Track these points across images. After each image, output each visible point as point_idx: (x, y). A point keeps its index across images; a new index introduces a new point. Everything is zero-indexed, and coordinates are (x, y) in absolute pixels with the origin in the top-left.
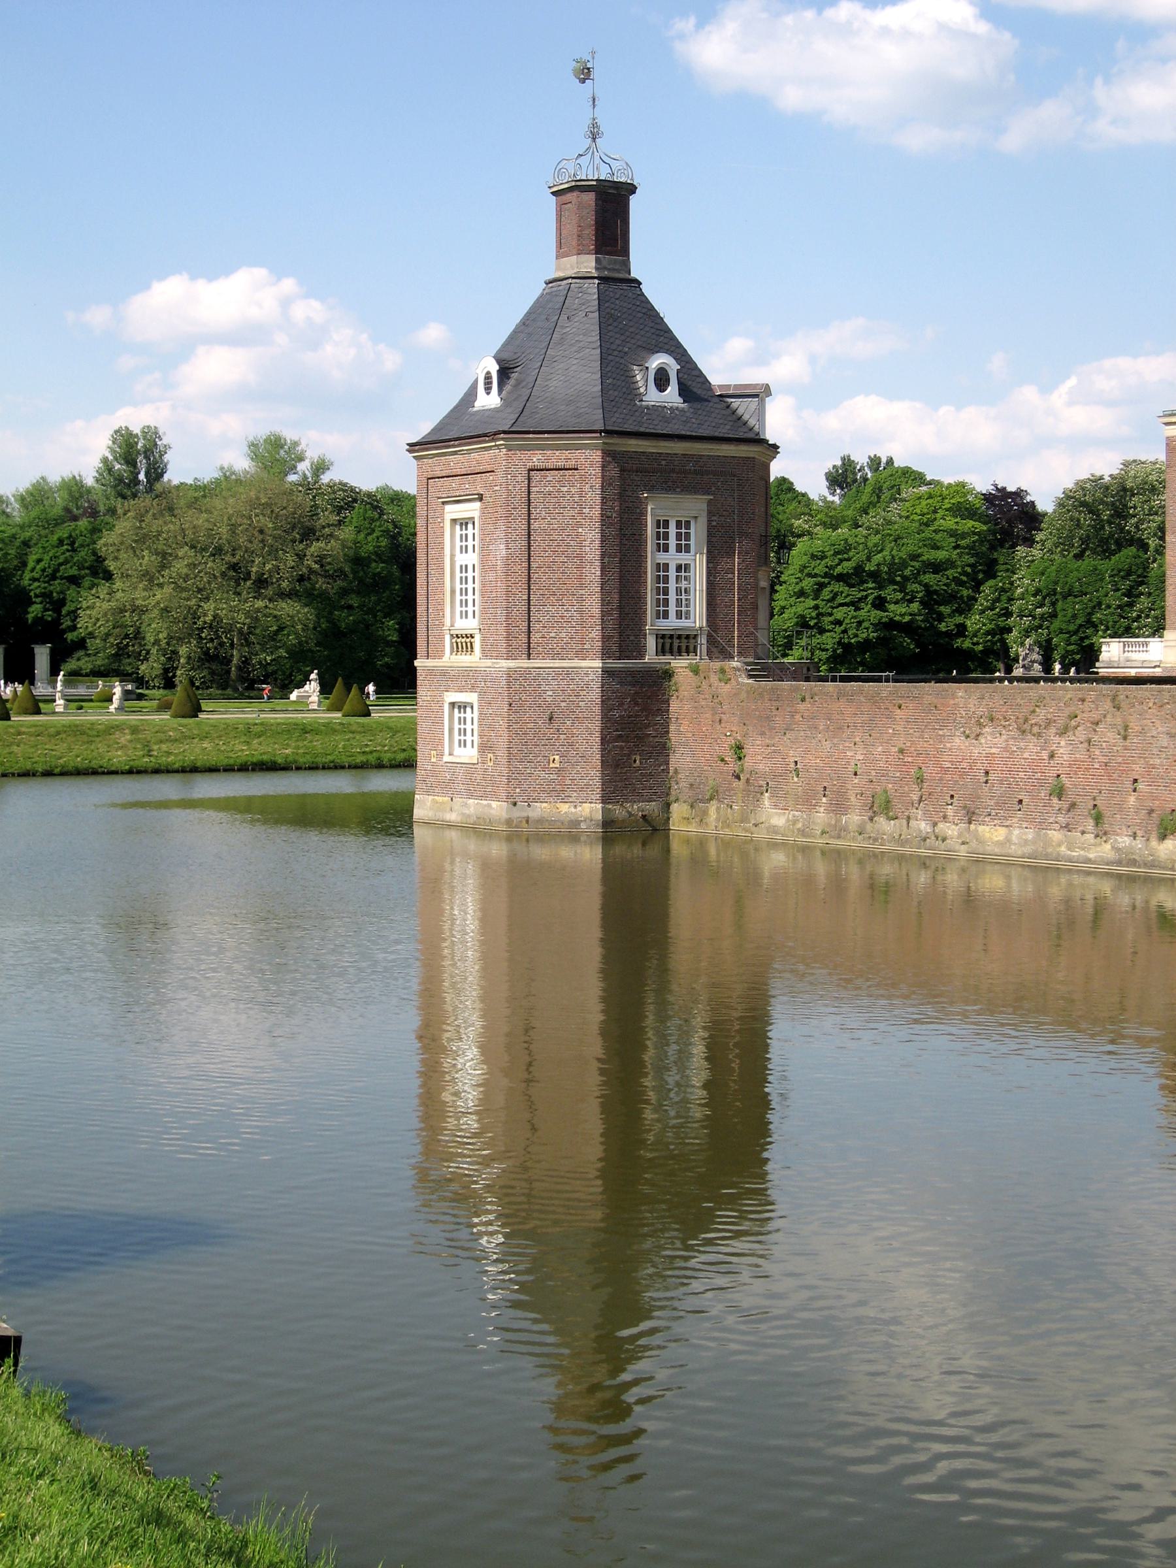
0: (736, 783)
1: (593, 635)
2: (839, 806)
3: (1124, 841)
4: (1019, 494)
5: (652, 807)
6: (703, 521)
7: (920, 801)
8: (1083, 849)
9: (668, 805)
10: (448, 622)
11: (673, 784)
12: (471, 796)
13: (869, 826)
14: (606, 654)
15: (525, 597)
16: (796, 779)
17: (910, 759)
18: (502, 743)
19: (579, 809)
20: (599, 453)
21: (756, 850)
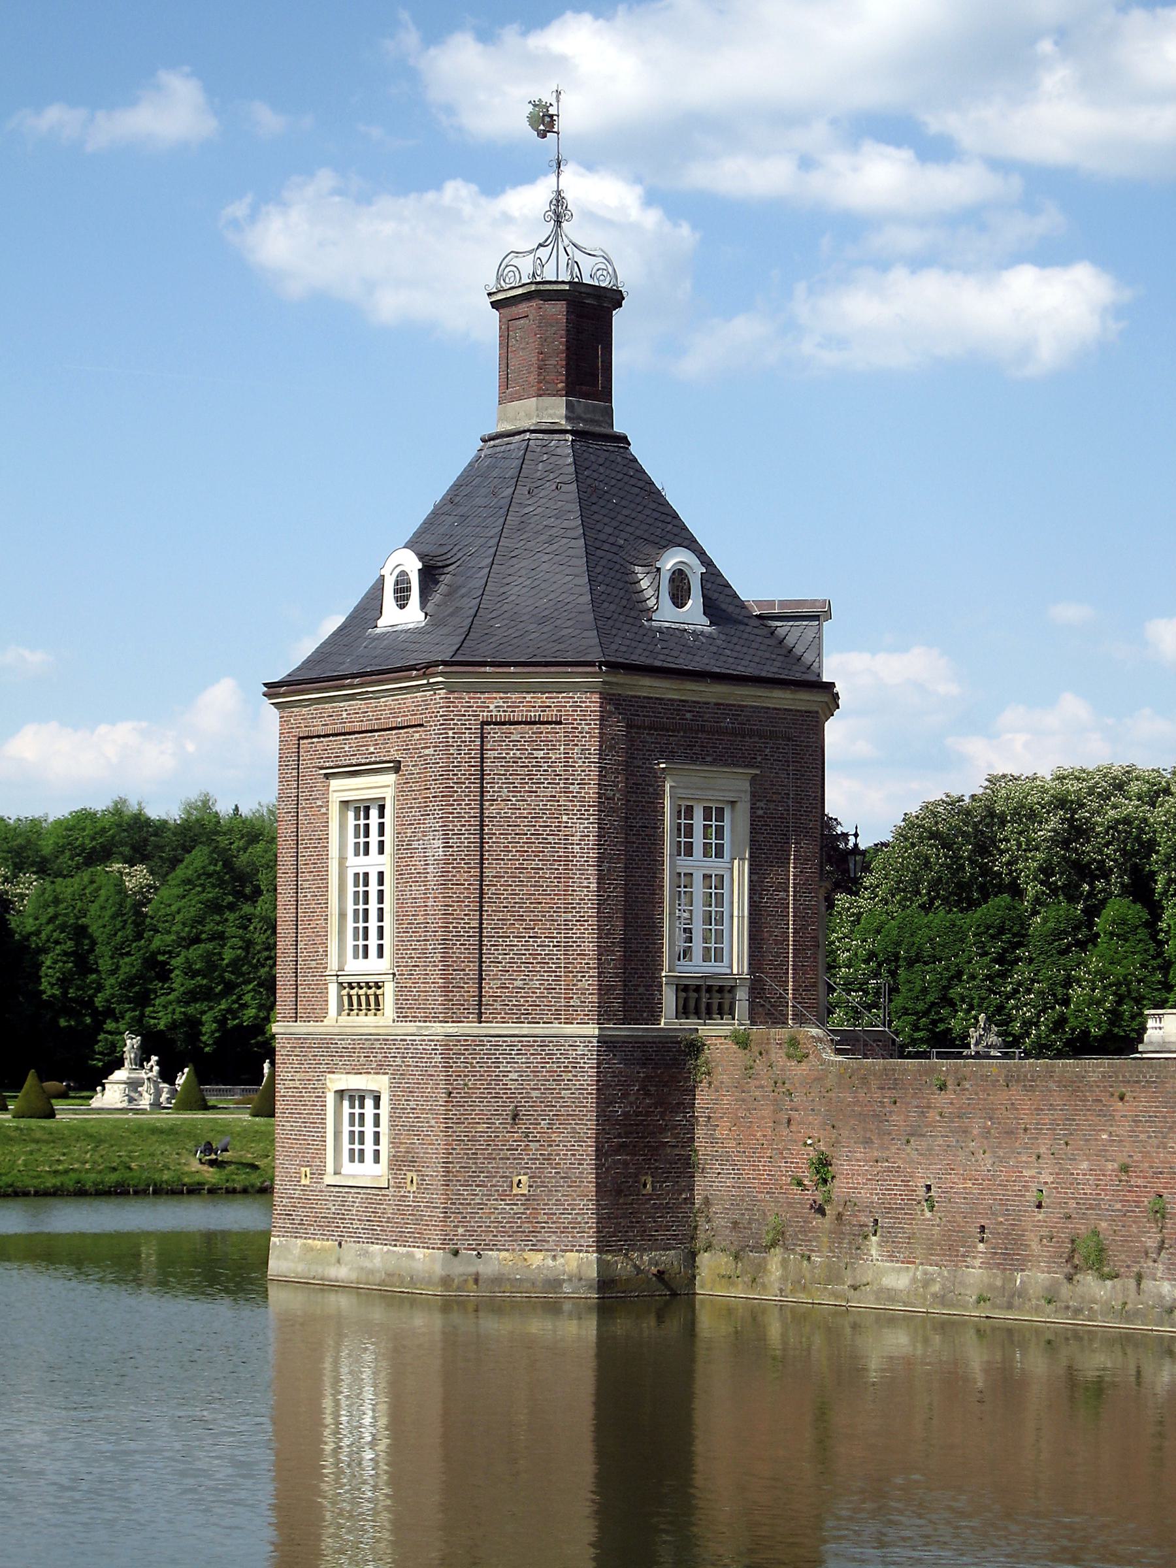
0: (817, 1221)
2: (1010, 1255)
5: (669, 1258)
6: (744, 808)
7: (1161, 1248)
9: (693, 1255)
10: (333, 963)
11: (701, 1221)
12: (376, 1240)
13: (1065, 1290)
14: (604, 1014)
16: (928, 1215)
17: (1140, 1182)
18: (433, 1153)
19: (560, 1261)
20: (596, 697)
21: (855, 1326)
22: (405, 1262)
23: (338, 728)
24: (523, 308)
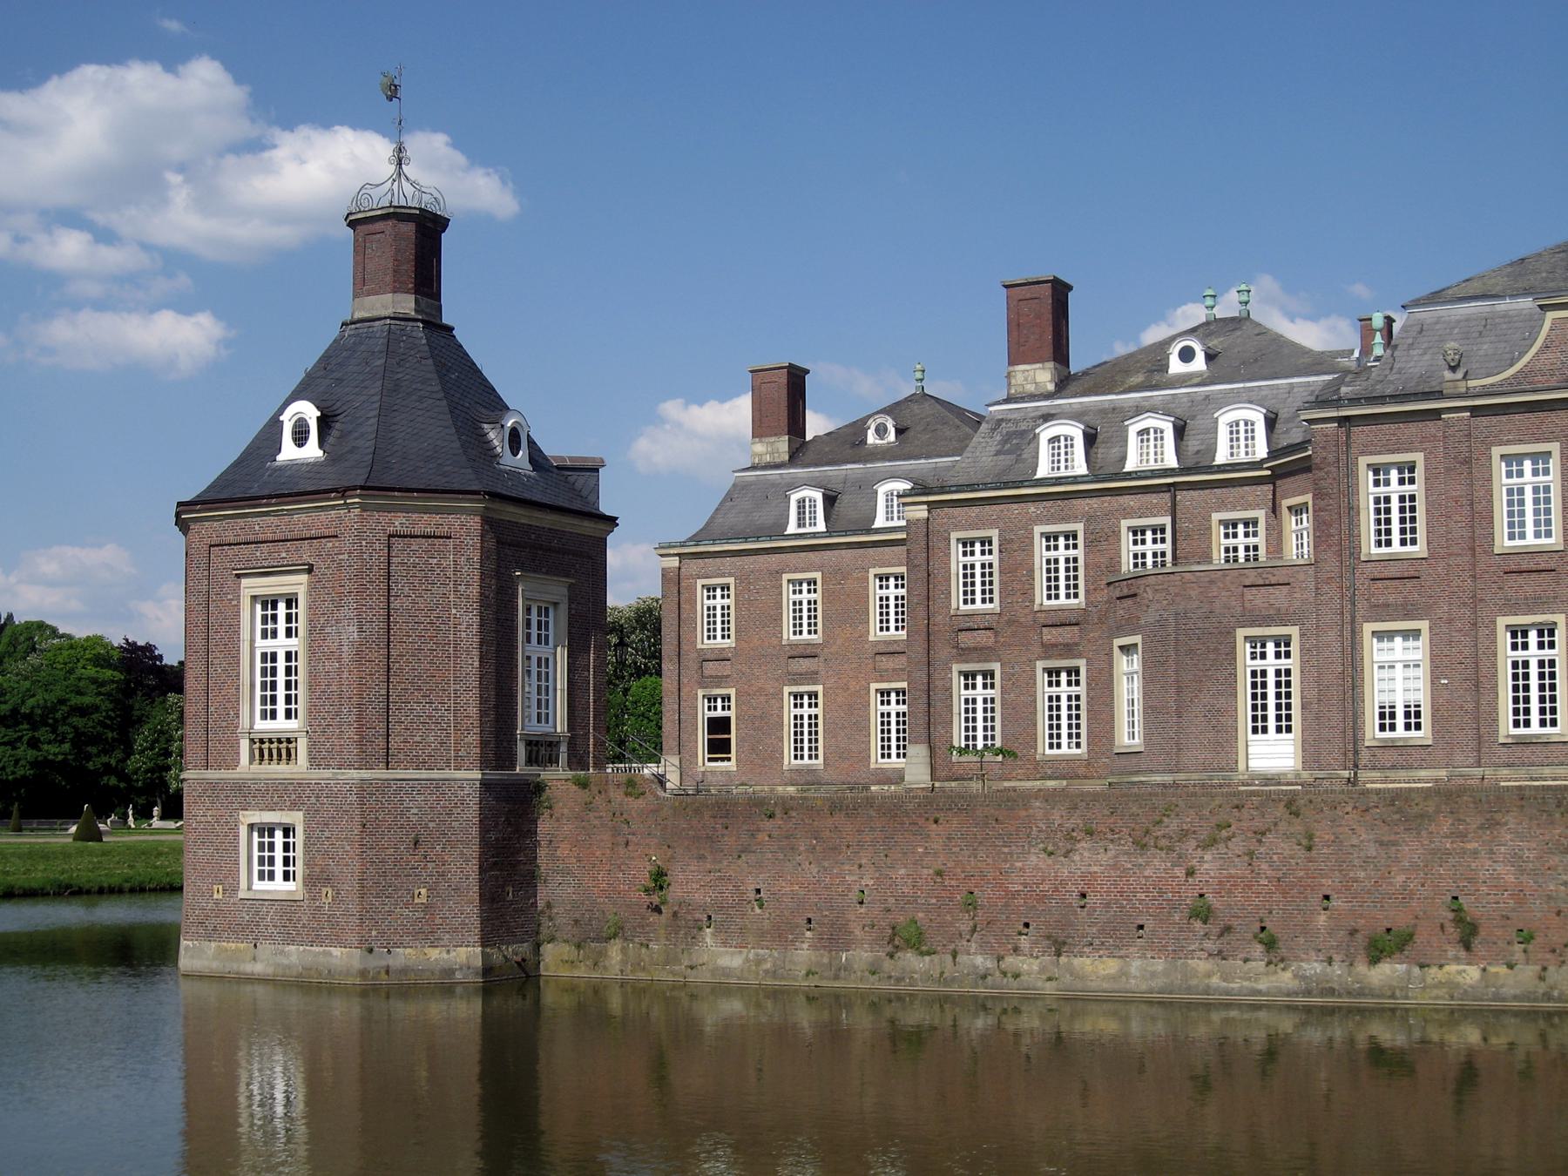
0: (654, 918)
1: (469, 739)
2: (835, 938)
3: (1314, 967)
4: (149, 648)
5: (524, 949)
6: (564, 607)
7: (974, 930)
8: (1249, 979)
9: (538, 945)
10: (244, 722)
11: (544, 920)
12: (293, 942)
13: (887, 964)
14: (484, 764)
15: (384, 692)
16: (758, 911)
17: (953, 883)
18: (349, 871)
19: (453, 954)
20: (478, 519)
21: (693, 997)
22: (321, 959)
23: (251, 538)
24: (379, 226)
